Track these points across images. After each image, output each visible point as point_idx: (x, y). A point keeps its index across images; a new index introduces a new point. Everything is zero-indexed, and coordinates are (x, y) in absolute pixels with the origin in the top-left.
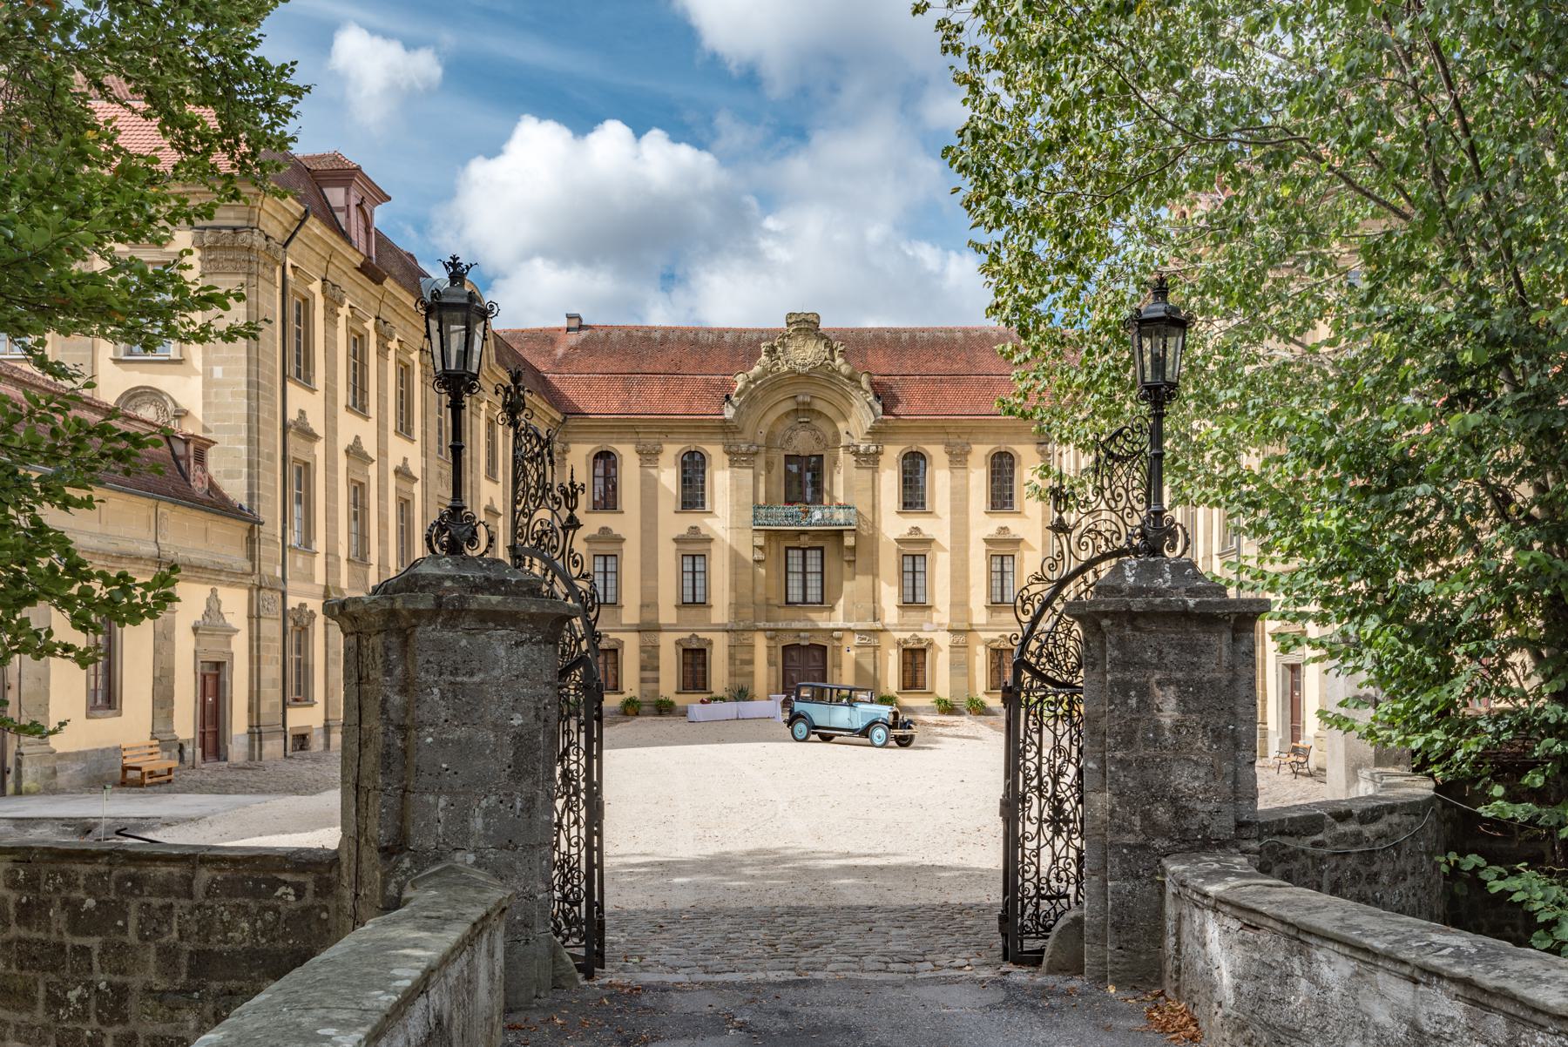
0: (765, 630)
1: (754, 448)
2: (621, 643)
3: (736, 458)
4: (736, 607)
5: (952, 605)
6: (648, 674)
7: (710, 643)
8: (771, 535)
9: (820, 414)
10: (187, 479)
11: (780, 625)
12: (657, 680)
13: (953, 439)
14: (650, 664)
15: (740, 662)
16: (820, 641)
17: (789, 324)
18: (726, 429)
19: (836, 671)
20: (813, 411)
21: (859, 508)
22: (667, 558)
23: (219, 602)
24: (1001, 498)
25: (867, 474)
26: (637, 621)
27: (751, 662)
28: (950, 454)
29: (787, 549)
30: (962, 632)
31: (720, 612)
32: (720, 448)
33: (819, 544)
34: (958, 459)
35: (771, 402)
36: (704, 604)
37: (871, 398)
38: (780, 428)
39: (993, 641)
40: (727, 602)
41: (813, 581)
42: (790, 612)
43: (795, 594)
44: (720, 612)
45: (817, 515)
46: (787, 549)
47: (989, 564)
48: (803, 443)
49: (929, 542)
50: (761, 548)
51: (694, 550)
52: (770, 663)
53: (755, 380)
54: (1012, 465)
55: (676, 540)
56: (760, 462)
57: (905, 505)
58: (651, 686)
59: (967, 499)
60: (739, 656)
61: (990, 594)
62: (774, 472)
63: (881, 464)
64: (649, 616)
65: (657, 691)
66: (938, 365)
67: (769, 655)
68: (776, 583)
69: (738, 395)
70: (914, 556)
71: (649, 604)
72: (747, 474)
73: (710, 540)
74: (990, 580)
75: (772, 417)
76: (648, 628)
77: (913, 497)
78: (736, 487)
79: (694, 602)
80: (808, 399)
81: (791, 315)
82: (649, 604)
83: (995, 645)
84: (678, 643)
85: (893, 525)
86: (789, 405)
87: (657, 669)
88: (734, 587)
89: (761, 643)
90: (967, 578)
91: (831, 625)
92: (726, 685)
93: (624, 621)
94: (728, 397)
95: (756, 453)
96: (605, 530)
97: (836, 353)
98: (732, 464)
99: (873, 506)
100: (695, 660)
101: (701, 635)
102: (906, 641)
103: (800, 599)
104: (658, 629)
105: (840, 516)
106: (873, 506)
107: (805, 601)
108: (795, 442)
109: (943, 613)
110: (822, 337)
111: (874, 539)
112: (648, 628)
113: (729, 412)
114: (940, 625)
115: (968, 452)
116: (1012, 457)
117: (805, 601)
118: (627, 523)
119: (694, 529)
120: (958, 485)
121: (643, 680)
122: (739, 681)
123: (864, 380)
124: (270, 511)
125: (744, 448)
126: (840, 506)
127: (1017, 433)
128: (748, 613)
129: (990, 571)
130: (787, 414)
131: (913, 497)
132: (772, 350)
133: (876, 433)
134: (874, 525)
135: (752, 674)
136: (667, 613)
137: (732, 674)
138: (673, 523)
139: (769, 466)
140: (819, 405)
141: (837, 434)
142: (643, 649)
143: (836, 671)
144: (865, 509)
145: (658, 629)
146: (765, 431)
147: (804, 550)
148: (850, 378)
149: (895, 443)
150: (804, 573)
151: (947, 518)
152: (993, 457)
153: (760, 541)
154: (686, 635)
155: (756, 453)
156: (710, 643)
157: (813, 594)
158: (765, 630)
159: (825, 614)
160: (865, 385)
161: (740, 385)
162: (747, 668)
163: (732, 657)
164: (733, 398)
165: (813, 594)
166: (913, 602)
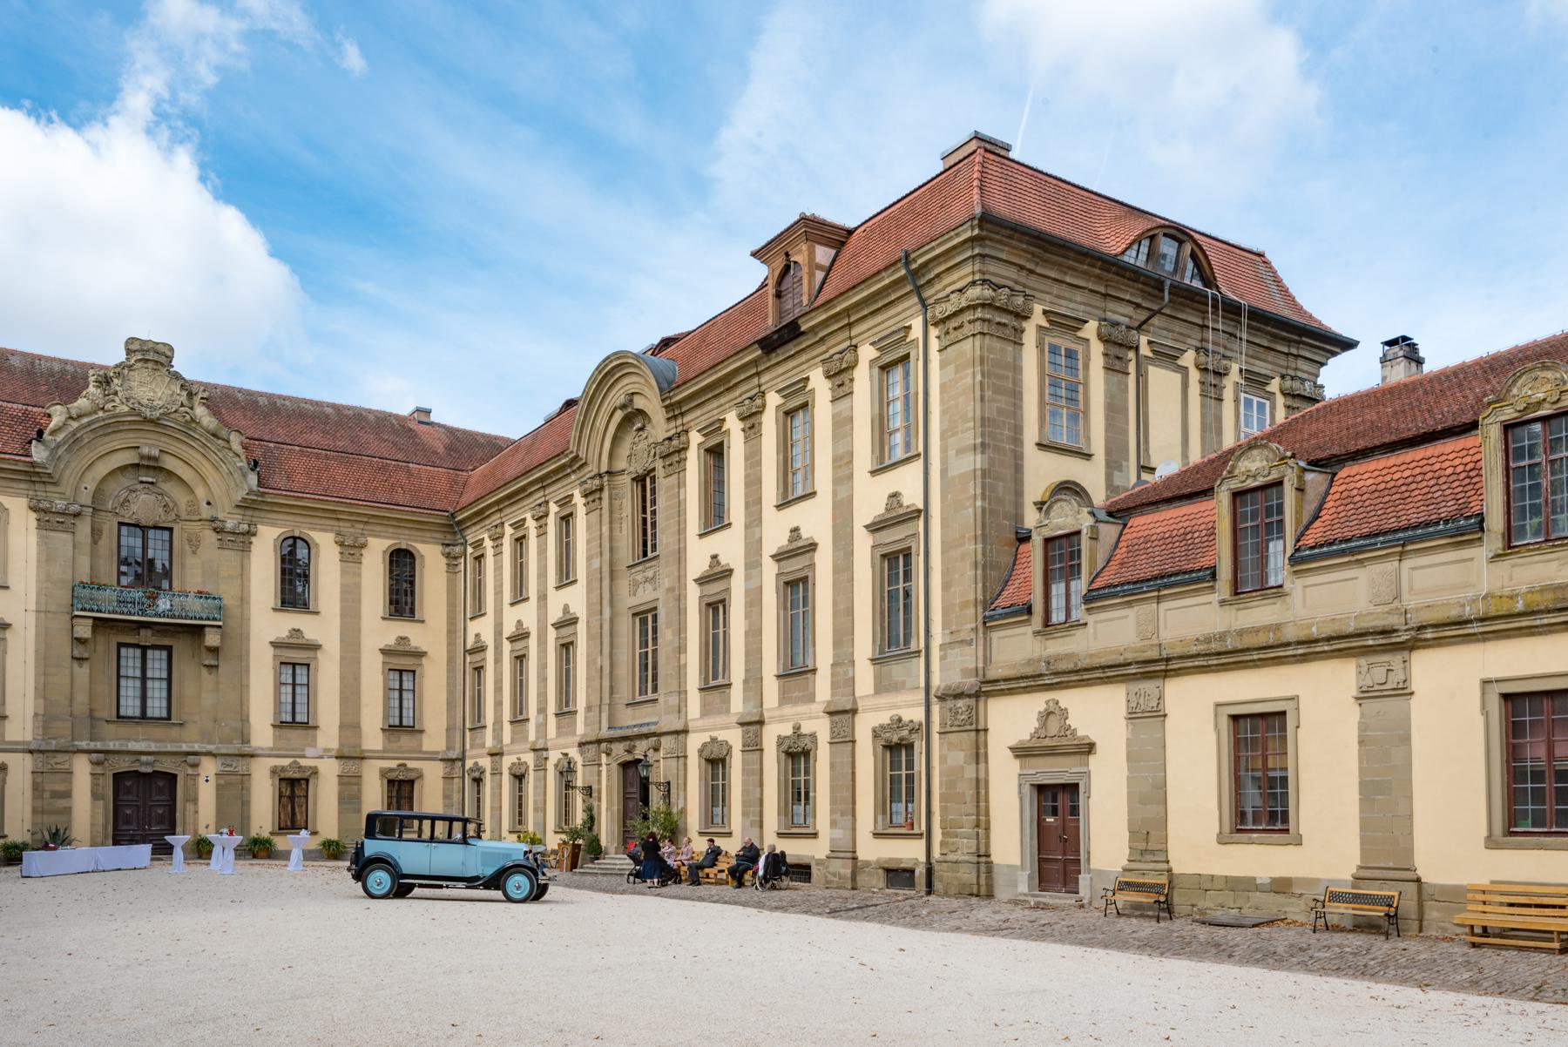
0: (89, 752)
1: (75, 508)
4: (45, 719)
5: (341, 727)
8: (100, 624)
9: (170, 474)
11: (111, 746)
13: (345, 528)
15: (50, 793)
16: (166, 766)
17: (129, 352)
19: (190, 807)
20: (161, 469)
21: (225, 601)
24: (402, 602)
25: (230, 556)
27: (68, 794)
28: (342, 544)
29: (120, 645)
30: (351, 756)
32: (24, 502)
33: (166, 642)
34: (351, 551)
35: (102, 450)
37: (244, 464)
38: (117, 488)
39: (392, 770)
40: (30, 712)
41: (157, 692)
42: (123, 730)
43: (131, 706)
45: (163, 604)
46: (120, 645)
48: (144, 506)
49: (315, 647)
50: (81, 641)
52: (95, 796)
53: (80, 416)
54: (413, 565)
56: (84, 528)
57: (283, 603)
59: (359, 601)
60: (49, 787)
61: (386, 716)
62: (103, 542)
63: (253, 548)
66: (315, 438)
67: (94, 785)
68: (105, 689)
69: (53, 433)
70: (296, 659)
72: (62, 539)
74: (387, 699)
75: (102, 469)
78: (47, 557)
80: (155, 452)
81: (131, 341)
83: (392, 776)
85: (266, 624)
86: (129, 458)
88: (42, 691)
89: (82, 769)
90: (358, 694)
91: (185, 748)
92: (28, 825)
94: (40, 433)
95: (77, 515)
97: (197, 399)
98: (42, 525)
99: (242, 599)
102: (283, 769)
103: (137, 713)
105: (195, 605)
106: (242, 599)
107: (144, 716)
108: (134, 508)
109: (329, 735)
110: (177, 376)
111: (244, 637)
113: (38, 453)
114: (326, 750)
115: (363, 546)
116: (412, 556)
117: (144, 716)
120: (347, 577)
122: (51, 821)
123: (236, 441)
125: (60, 504)
126: (200, 594)
129: (388, 689)
130: (123, 469)
132: (105, 382)
133: (246, 506)
134: (244, 621)
135: (68, 811)
137: (35, 811)
139: (96, 534)
141: (194, 504)
143: (190, 807)
144: (229, 601)
146: (92, 487)
147: (144, 649)
148: (214, 435)
149: (274, 525)
150: (144, 679)
151: (336, 622)
152: (391, 555)
153: (84, 630)
155: (77, 515)
157: (156, 707)
158: (89, 752)
159: (175, 731)
160: (236, 447)
161: (56, 421)
162: (61, 803)
163: (37, 788)
164: (46, 436)
165: (156, 707)
166: (295, 722)
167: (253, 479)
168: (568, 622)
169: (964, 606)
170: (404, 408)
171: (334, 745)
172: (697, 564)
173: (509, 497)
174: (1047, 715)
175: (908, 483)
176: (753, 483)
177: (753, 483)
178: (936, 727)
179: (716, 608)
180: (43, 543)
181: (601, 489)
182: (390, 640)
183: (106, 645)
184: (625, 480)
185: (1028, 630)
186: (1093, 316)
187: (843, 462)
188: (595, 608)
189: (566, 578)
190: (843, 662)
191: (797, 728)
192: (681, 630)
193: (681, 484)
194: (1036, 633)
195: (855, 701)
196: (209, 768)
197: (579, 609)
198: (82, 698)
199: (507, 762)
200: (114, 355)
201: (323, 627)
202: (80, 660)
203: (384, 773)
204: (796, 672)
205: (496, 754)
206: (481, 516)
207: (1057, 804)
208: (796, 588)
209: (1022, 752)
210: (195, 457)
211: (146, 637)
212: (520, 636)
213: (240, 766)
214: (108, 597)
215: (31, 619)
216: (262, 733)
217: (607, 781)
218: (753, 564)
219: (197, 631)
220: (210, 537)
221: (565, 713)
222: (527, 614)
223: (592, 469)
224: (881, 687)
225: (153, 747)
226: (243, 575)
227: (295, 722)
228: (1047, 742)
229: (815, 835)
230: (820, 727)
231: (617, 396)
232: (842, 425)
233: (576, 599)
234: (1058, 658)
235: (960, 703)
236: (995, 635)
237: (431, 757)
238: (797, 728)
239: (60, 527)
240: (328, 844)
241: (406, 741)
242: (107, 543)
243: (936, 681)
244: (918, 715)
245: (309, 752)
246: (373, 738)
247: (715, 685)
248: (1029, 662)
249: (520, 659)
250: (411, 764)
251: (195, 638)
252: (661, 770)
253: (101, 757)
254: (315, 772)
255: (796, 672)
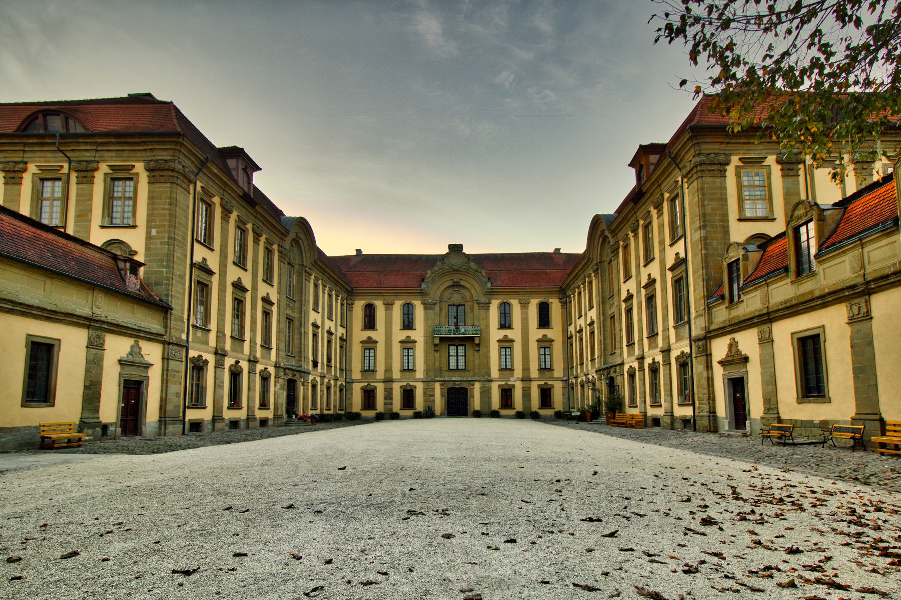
2: (376, 388)
3: (427, 307)
4: (427, 371)
6: (388, 401)
7: (415, 387)
8: (442, 339)
9: (463, 287)
10: (124, 281)
12: (392, 404)
13: (522, 297)
14: (389, 396)
15: (429, 395)
16: (464, 385)
18: (422, 294)
22: (397, 349)
23: (140, 349)
24: (544, 321)
26: (383, 378)
27: (434, 396)
30: (526, 380)
31: (420, 374)
36: (413, 371)
41: (461, 361)
42: (451, 374)
43: (453, 366)
44: (420, 374)
47: (539, 352)
48: (456, 299)
49: (512, 341)
50: (436, 345)
51: (408, 345)
52: (442, 396)
55: (400, 342)
58: (389, 407)
61: (539, 365)
64: (388, 375)
65: (391, 409)
68: (444, 360)
71: (389, 370)
73: (416, 342)
74: (539, 359)
75: (442, 288)
76: (388, 381)
77: (505, 324)
78: (427, 319)
79: (408, 370)
82: (389, 370)
84: (401, 387)
85: (495, 334)
87: (392, 399)
88: (426, 362)
89: (438, 387)
93: (378, 378)
96: (369, 338)
98: (426, 309)
100: (408, 396)
101: (412, 384)
104: (392, 381)
111: (488, 340)
112: (388, 381)
118: (378, 335)
119: (408, 337)
121: (386, 404)
122: (428, 404)
124: (181, 300)
125: (430, 301)
127: (550, 293)
128: (432, 374)
129: (539, 355)
130: (449, 287)
131: (505, 324)
135: (434, 401)
136: (396, 375)
137: (425, 401)
138: (400, 335)
139: (441, 309)
140: (462, 283)
142: (386, 390)
145: (392, 381)
150: (457, 356)
154: (405, 384)
156: (415, 387)
160: (484, 274)
162: (432, 399)
163: (425, 394)
167: (489, 285)
168: (592, 323)
169: (700, 300)
170: (551, 250)
171: (520, 377)
172: (624, 296)
173: (574, 277)
174: (730, 346)
175: (680, 247)
176: (637, 258)
177: (637, 258)
178: (694, 355)
179: (629, 311)
180: (426, 314)
181: (598, 269)
182: (540, 337)
183: (444, 347)
184: (606, 264)
185: (723, 307)
186: (771, 154)
187: (662, 242)
188: (599, 316)
189: (591, 308)
190: (666, 330)
191: (653, 360)
192: (620, 322)
193: (618, 263)
194: (727, 308)
195: (669, 346)
196: (477, 386)
197: (595, 319)
198: (438, 363)
199: (579, 380)
200: (445, 251)
201: (514, 334)
202: (437, 351)
203: (539, 386)
204: (653, 335)
205: (576, 378)
206: (568, 286)
207: (737, 387)
208: (651, 299)
209: (722, 363)
210: (471, 281)
211: (457, 343)
212: (581, 331)
213: (487, 384)
214: (444, 330)
215: (423, 339)
216: (495, 373)
217: (602, 386)
218: (639, 292)
219: (472, 339)
220: (476, 306)
221: (593, 360)
222: (581, 322)
223: (594, 262)
224: (678, 338)
225: (459, 379)
226: (487, 318)
227: (506, 370)
228: (730, 359)
229: (660, 406)
230: (659, 358)
231: (599, 233)
232: (661, 227)
233: (593, 314)
234: (733, 318)
235: (700, 343)
236: (714, 310)
237: (557, 380)
238: (653, 360)
239: (430, 309)
240: (518, 413)
241: (547, 373)
242: (445, 313)
243: (694, 334)
244: (687, 350)
245: (511, 379)
246: (534, 373)
247: (630, 345)
248: (724, 322)
249: (581, 339)
250: (549, 383)
251: (472, 343)
252: (618, 381)
253: (443, 383)
254: (513, 386)
255: (653, 335)
